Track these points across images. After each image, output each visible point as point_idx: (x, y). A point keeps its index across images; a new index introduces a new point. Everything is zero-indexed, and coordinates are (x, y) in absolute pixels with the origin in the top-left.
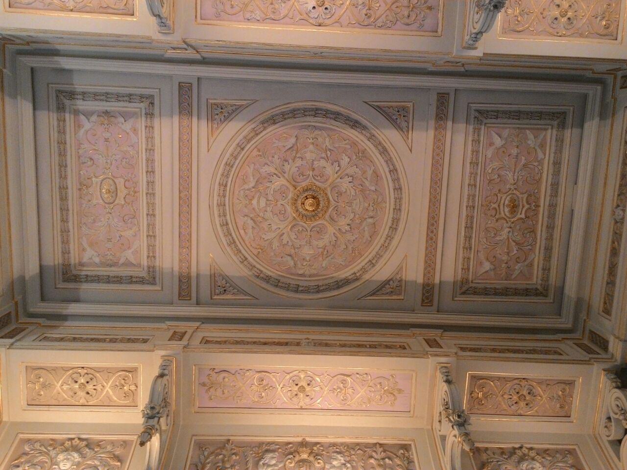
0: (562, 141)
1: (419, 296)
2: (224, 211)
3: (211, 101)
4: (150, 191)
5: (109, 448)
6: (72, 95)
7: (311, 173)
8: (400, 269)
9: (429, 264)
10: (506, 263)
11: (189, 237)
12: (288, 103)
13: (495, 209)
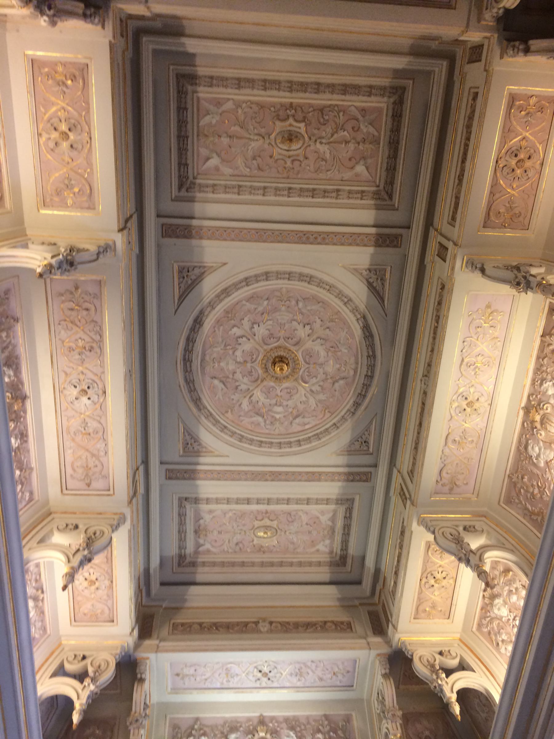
0: (212, 78)
1: (391, 250)
2: (285, 443)
3: (181, 452)
4: (266, 502)
5: (497, 573)
6: (181, 557)
7: (249, 365)
8: (356, 271)
9: (353, 240)
10: (359, 143)
12: (180, 386)
13: (293, 161)
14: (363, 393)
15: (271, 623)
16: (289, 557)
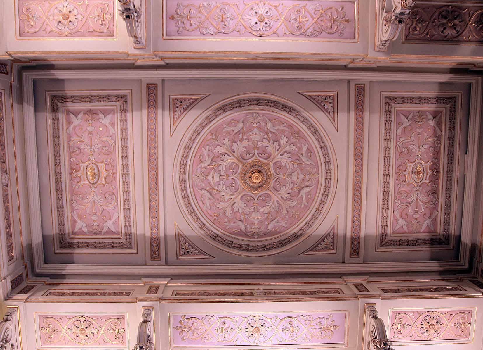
4: (125, 172)
6: (63, 99)
7: (256, 152)
9: (356, 223)
11: (157, 209)
12: (236, 96)
14: (233, 245)
15: (7, 186)
16: (66, 196)
